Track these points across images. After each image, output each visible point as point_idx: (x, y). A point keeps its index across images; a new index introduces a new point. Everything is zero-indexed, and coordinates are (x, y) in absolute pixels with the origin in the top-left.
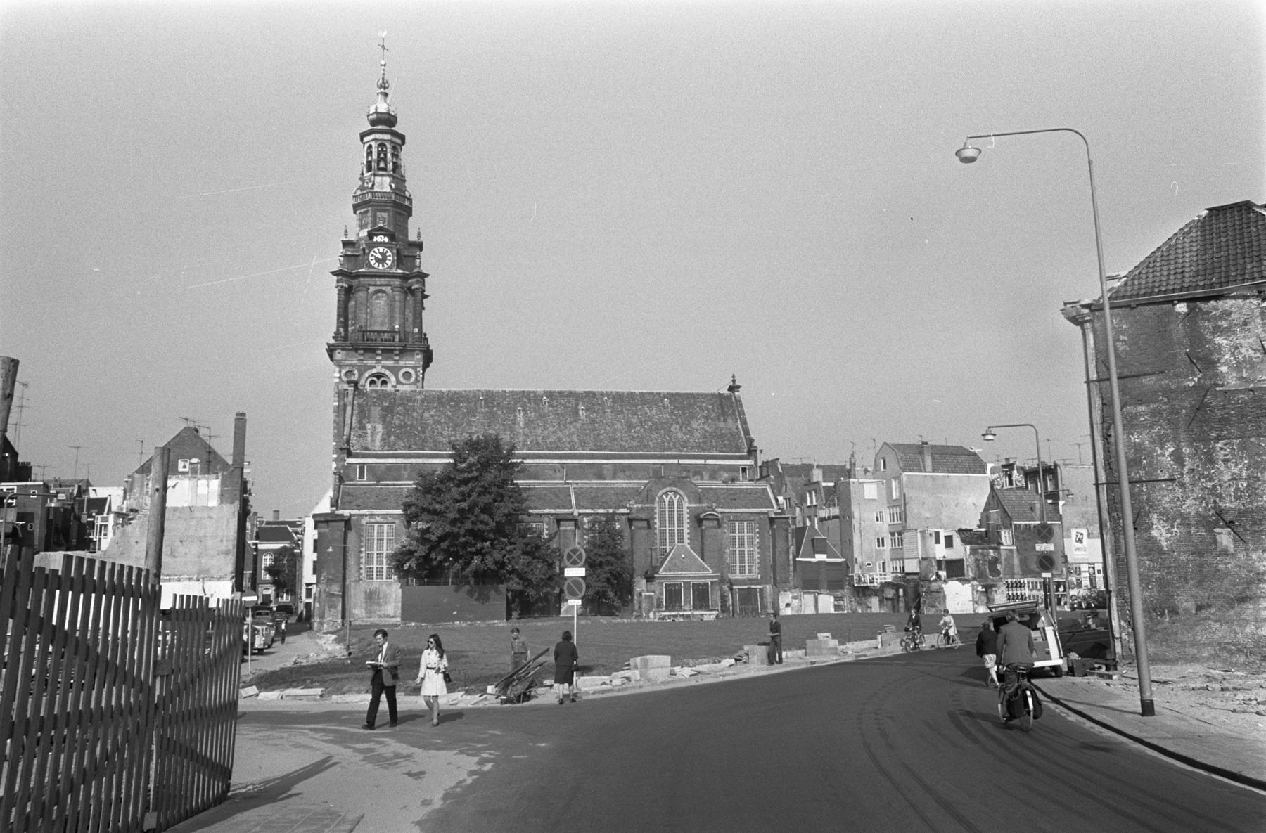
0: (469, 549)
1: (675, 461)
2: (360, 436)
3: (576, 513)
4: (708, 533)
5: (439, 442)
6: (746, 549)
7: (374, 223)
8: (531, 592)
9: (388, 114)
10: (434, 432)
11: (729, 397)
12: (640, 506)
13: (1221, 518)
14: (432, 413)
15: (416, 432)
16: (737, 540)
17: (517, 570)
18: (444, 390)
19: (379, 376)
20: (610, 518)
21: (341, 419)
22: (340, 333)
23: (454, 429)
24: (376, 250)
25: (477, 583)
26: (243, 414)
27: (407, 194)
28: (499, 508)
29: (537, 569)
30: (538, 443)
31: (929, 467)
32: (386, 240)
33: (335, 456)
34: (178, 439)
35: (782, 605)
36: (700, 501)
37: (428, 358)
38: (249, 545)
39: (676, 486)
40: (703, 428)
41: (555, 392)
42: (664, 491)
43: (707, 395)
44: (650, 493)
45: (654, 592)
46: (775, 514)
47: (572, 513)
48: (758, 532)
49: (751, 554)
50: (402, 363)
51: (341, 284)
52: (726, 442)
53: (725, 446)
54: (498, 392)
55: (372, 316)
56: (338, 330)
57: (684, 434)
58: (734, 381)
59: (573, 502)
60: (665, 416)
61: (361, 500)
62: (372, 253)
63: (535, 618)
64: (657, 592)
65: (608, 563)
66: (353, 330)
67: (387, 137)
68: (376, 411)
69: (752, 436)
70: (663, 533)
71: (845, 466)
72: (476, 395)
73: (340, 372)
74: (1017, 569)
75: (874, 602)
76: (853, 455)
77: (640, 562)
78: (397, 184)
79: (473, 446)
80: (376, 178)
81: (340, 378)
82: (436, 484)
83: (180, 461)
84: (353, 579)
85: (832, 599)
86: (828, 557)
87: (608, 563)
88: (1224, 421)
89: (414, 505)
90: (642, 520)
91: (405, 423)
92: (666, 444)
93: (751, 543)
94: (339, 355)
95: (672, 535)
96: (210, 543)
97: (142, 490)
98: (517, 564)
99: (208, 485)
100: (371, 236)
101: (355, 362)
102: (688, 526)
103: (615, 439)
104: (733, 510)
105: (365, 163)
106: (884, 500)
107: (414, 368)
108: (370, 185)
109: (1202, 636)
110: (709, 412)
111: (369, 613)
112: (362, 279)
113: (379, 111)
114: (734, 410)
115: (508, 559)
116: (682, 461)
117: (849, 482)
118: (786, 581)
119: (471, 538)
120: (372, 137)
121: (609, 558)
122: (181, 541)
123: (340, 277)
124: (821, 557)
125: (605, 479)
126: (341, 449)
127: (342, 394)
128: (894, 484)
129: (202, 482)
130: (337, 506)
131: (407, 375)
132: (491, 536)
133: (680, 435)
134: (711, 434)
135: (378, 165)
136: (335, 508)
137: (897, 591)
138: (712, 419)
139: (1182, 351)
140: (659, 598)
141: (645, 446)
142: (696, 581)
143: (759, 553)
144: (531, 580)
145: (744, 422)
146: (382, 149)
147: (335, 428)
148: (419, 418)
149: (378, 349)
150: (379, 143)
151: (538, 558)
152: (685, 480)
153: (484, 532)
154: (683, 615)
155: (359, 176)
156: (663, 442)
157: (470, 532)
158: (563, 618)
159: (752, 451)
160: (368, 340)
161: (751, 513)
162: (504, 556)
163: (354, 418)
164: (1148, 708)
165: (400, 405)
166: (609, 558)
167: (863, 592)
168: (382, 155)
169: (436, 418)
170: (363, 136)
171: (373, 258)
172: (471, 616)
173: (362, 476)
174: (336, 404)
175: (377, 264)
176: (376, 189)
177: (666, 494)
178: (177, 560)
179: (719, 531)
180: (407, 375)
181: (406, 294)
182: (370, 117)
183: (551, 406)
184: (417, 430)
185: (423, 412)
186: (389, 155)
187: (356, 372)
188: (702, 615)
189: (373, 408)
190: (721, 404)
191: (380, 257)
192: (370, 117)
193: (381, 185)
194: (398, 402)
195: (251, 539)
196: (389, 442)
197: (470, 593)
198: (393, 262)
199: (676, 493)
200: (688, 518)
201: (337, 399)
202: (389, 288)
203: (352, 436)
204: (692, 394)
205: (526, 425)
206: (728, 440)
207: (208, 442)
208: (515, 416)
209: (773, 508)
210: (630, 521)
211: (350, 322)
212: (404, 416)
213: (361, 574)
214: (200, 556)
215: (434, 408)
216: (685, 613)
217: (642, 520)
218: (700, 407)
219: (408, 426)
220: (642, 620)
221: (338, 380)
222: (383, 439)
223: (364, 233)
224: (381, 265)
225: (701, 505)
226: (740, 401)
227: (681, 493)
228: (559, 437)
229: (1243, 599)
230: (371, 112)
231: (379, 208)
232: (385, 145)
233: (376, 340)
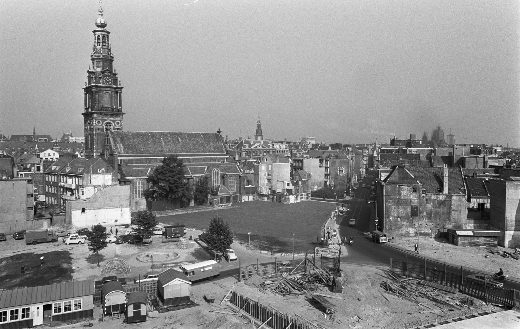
1: (209, 157)
6: (233, 184)
11: (218, 135)
13: (399, 217)
18: (138, 131)
23: (144, 146)
30: (170, 151)
31: (278, 162)
36: (223, 171)
49: (234, 185)
50: (116, 119)
54: (154, 133)
58: (219, 130)
68: (118, 139)
70: (214, 180)
72: (148, 133)
73: (96, 122)
74: (302, 191)
75: (266, 199)
81: (96, 124)
85: (252, 196)
88: (401, 203)
93: (234, 183)
95: (216, 181)
96: (123, 197)
97: (87, 179)
101: (100, 118)
103: (191, 149)
106: (266, 170)
109: (395, 233)
111: (136, 208)
113: (102, 22)
116: (211, 157)
117: (258, 165)
118: (243, 193)
120: (100, 33)
124: (250, 186)
128: (270, 166)
129: (106, 176)
131: (118, 123)
133: (208, 148)
137: (274, 197)
139: (397, 192)
141: (199, 152)
154: (224, 205)
164: (418, 253)
165: (125, 137)
167: (262, 195)
168: (104, 41)
172: (171, 209)
177: (215, 170)
180: (118, 123)
183: (170, 138)
185: (133, 140)
187: (101, 122)
190: (217, 137)
194: (124, 136)
198: (111, 82)
199: (217, 169)
204: (208, 134)
214: (120, 201)
218: (211, 138)
222: (124, 150)
227: (218, 169)
228: (175, 149)
229: (400, 228)
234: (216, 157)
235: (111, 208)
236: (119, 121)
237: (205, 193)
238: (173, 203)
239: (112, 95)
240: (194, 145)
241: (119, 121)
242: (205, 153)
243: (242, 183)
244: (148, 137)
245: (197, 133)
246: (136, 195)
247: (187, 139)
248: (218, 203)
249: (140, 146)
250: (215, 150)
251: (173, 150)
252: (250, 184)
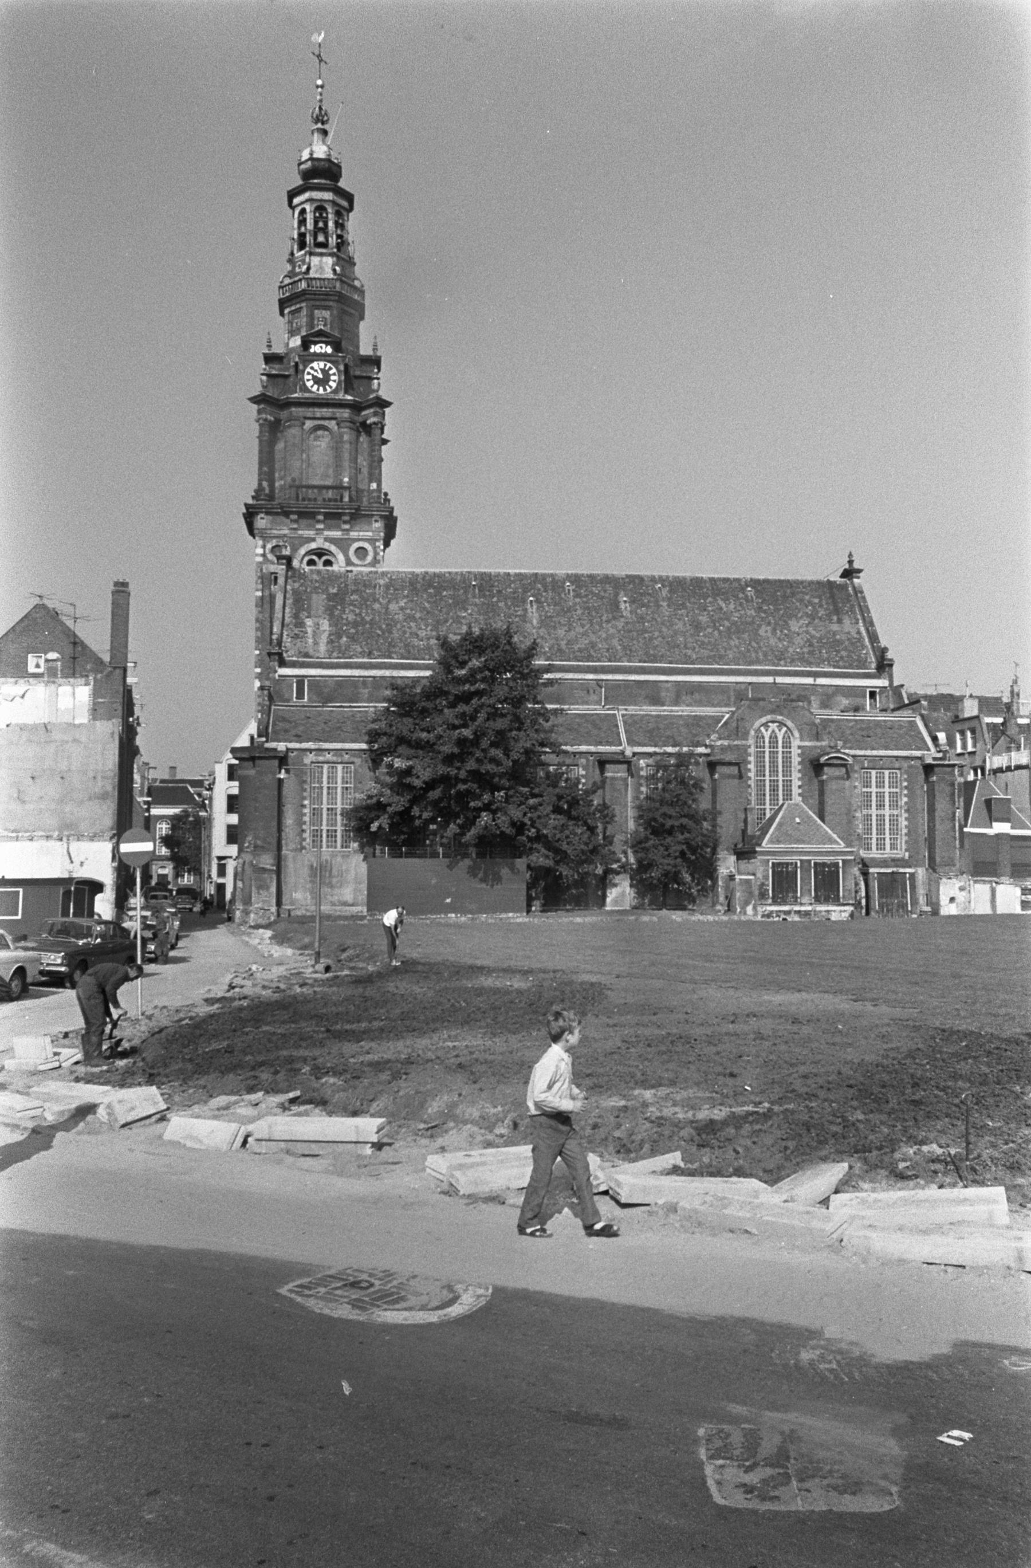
0: (472, 804)
1: (769, 679)
2: (296, 637)
3: (628, 753)
4: (832, 786)
5: (414, 647)
6: (887, 812)
7: (311, 324)
8: (564, 870)
9: (329, 160)
10: (405, 632)
11: (844, 587)
12: (726, 743)
14: (402, 603)
15: (379, 632)
16: (874, 798)
17: (546, 836)
19: (320, 553)
20: (683, 760)
21: (267, 615)
22: (263, 489)
24: (315, 365)
25: (481, 855)
26: (125, 584)
27: (357, 283)
28: (516, 740)
29: (575, 834)
30: (560, 650)
32: (329, 350)
33: (258, 670)
34: (26, 622)
35: (944, 900)
36: (817, 737)
37: (390, 534)
38: (139, 803)
39: (781, 714)
40: (807, 632)
41: (583, 575)
42: (763, 720)
43: (811, 583)
45: (754, 874)
46: (935, 759)
47: (623, 753)
48: (906, 787)
50: (354, 534)
51: (264, 416)
52: (844, 653)
53: (842, 658)
54: (498, 575)
55: (309, 465)
56: (260, 484)
57: (779, 639)
58: (851, 562)
59: (623, 737)
60: (749, 613)
61: (301, 728)
62: (308, 370)
63: (568, 911)
64: (759, 875)
65: (683, 828)
66: (281, 486)
67: (328, 196)
68: (319, 601)
69: (884, 643)
70: (760, 784)
71: (1000, 698)
73: (264, 547)
76: (1015, 682)
77: (728, 828)
78: (343, 268)
79: (475, 644)
80: (313, 258)
81: (264, 555)
82: (420, 701)
83: (30, 656)
84: (292, 846)
85: (1018, 891)
86: (1012, 828)
87: (683, 828)
89: (385, 734)
90: (730, 764)
91: (363, 619)
92: (753, 655)
93: (894, 805)
94: (262, 522)
95: (774, 789)
98: (545, 826)
99: (74, 694)
100: (306, 344)
101: (286, 532)
102: (800, 775)
104: (869, 753)
105: (296, 236)
107: (372, 541)
108: (304, 268)
110: (814, 607)
111: (318, 899)
112: (293, 409)
113: (315, 156)
114: (852, 606)
115: (531, 819)
116: (780, 680)
118: (951, 863)
119: (475, 786)
120: (307, 195)
121: (685, 821)
122: (33, 778)
123: (262, 406)
124: (1000, 828)
125: (663, 705)
126: (270, 654)
127: (268, 580)
129: (65, 690)
130: (267, 735)
131: (361, 552)
132: (505, 782)
134: (820, 640)
135: (315, 238)
136: (264, 739)
138: (820, 618)
140: (763, 884)
141: (721, 657)
142: (820, 859)
143: (906, 819)
144: (565, 852)
145: (869, 624)
146: (321, 214)
147: (257, 629)
148: (383, 611)
149: (319, 513)
150: (315, 205)
151: (576, 819)
152: (794, 704)
153: (494, 775)
154: (798, 912)
155: (287, 256)
156: (749, 651)
157: (475, 775)
158: (612, 912)
159: (884, 666)
160: (304, 499)
161: (897, 758)
162: (525, 814)
163: (287, 610)
165: (353, 592)
166: (685, 821)
168: (321, 225)
169: (408, 611)
170: (292, 195)
171: (310, 377)
172: (474, 906)
173: (300, 695)
174: (259, 594)
175: (316, 387)
176: (312, 274)
177: (765, 725)
178: (27, 806)
179: (847, 783)
180: (361, 552)
181: (359, 432)
182: (303, 167)
184: (380, 628)
185: (389, 602)
186: (331, 224)
188: (828, 912)
189: (314, 596)
191: (320, 376)
192: (303, 167)
193: (321, 268)
195: (142, 795)
196: (340, 647)
197: (472, 872)
198: (339, 384)
199: (782, 724)
200: (799, 763)
201: (260, 587)
202: (334, 422)
203: (285, 637)
205: (542, 622)
206: (845, 649)
207: (72, 627)
208: (526, 610)
209: (929, 750)
210: (712, 766)
211: (277, 475)
212: (361, 608)
213: (304, 840)
214: (61, 801)
215: (405, 597)
216: (803, 908)
217: (730, 764)
219: (367, 623)
220: (736, 918)
221: (260, 559)
222: (330, 642)
223: (296, 342)
224: (321, 389)
225: (818, 744)
226: (862, 592)
227: (789, 723)
228: (591, 643)
230: (303, 159)
231: (318, 303)
232: (325, 209)
233: (315, 500)
234: (809, 681)
235: (17, 839)
236: (366, 545)
237: (681, 837)
238: (481, 875)
239: (342, 437)
240: (697, 626)
241: (366, 545)
242: (750, 664)
243: (942, 805)
244: (466, 592)
245: (726, 580)
246: (316, 835)
247: (665, 604)
248: (763, 895)
249: (414, 629)
250: (810, 653)
251: (576, 647)
252: (998, 820)
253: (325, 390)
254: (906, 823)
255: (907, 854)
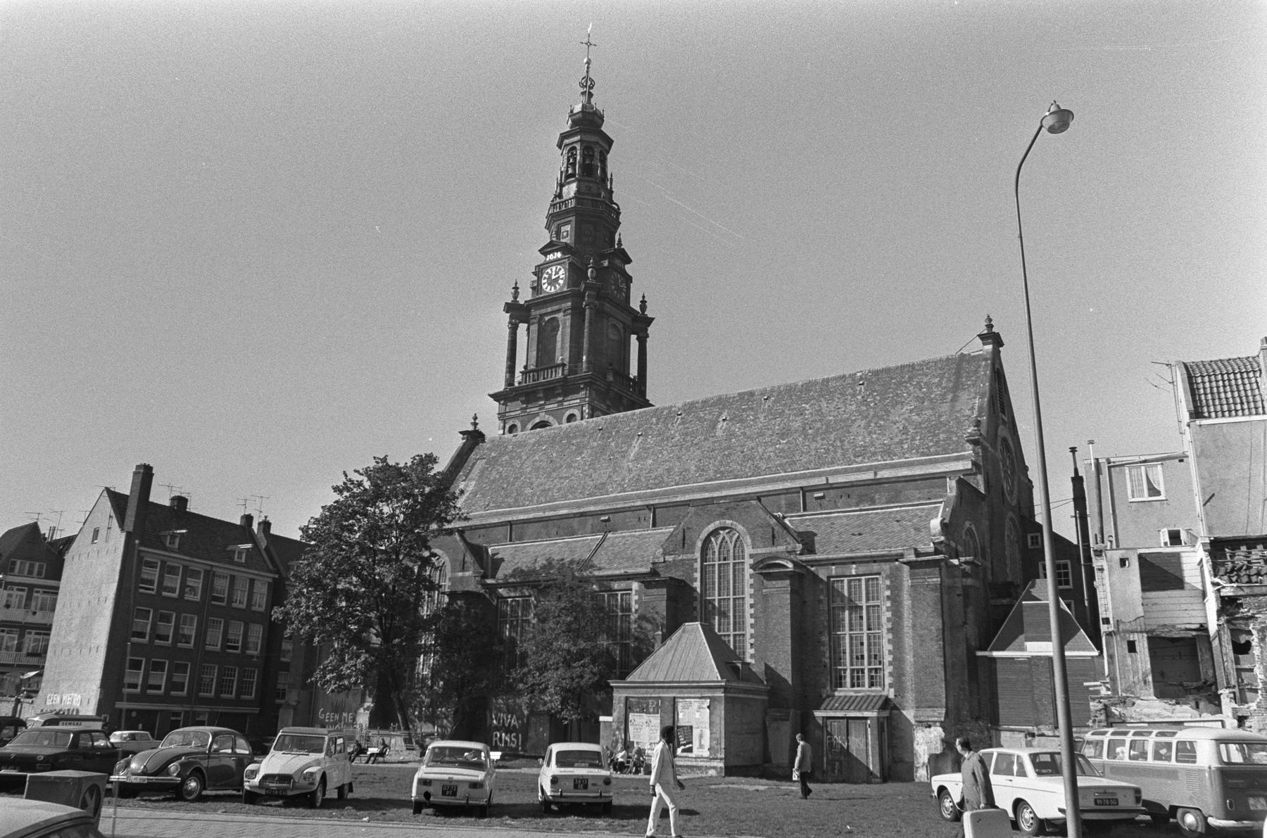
39: (731, 518)
42: (711, 527)
44: (688, 535)
152: (745, 504)
253: (555, 288)
254: (890, 647)
255: (892, 690)
